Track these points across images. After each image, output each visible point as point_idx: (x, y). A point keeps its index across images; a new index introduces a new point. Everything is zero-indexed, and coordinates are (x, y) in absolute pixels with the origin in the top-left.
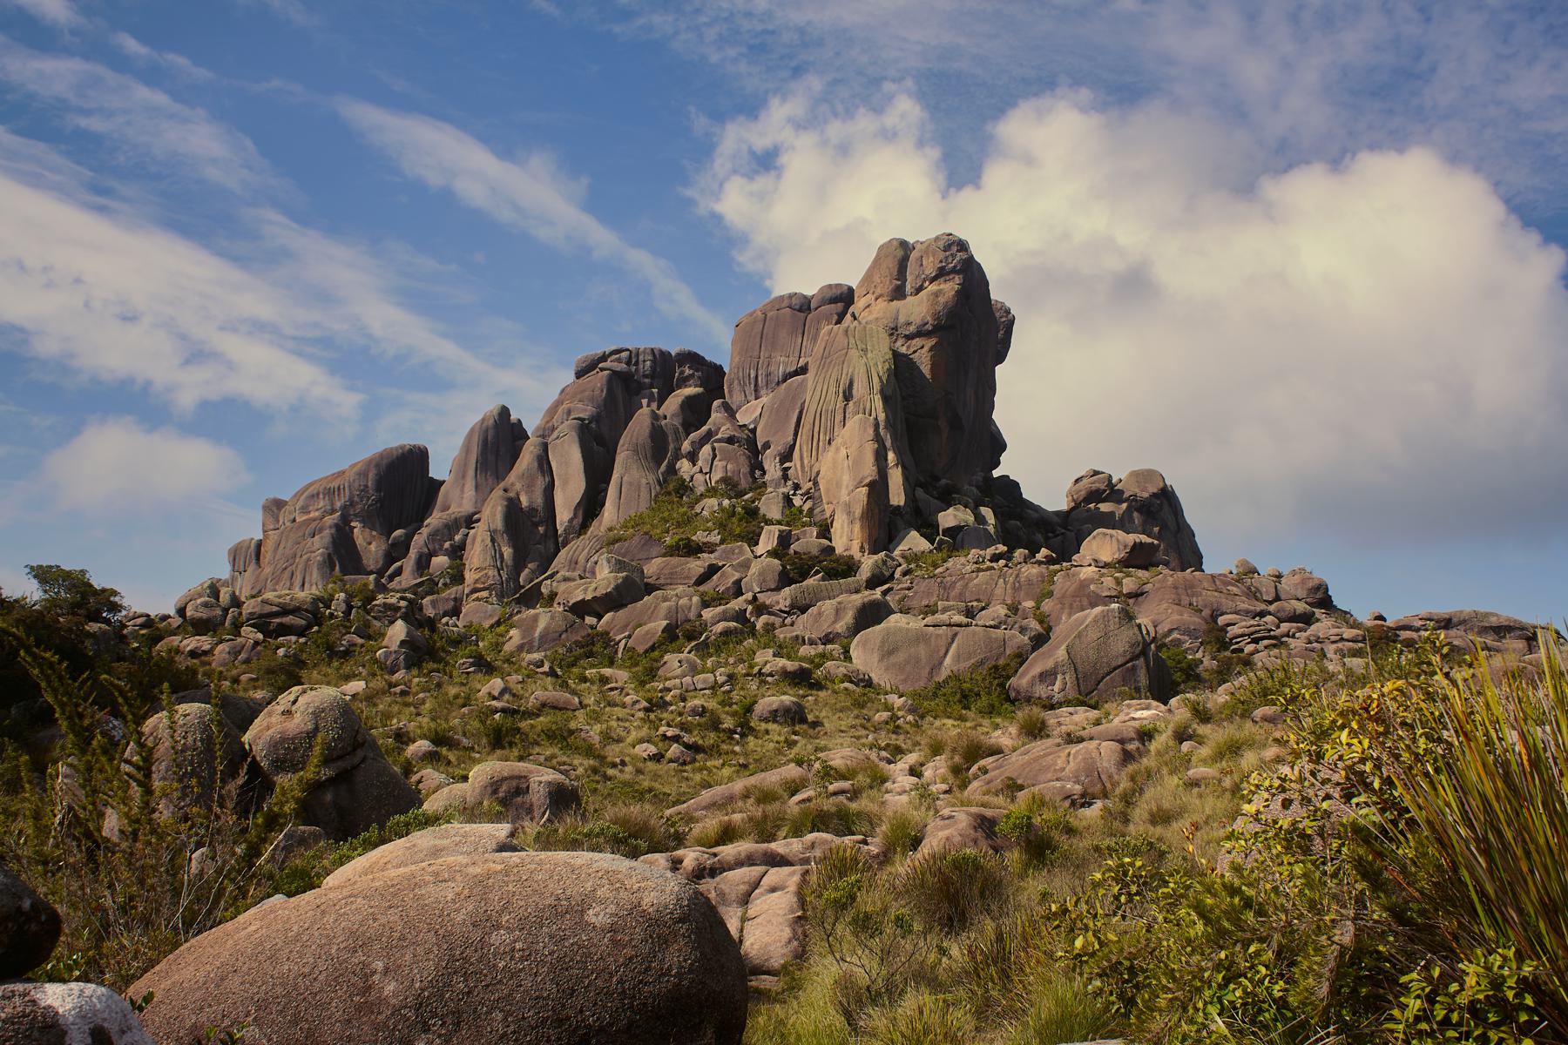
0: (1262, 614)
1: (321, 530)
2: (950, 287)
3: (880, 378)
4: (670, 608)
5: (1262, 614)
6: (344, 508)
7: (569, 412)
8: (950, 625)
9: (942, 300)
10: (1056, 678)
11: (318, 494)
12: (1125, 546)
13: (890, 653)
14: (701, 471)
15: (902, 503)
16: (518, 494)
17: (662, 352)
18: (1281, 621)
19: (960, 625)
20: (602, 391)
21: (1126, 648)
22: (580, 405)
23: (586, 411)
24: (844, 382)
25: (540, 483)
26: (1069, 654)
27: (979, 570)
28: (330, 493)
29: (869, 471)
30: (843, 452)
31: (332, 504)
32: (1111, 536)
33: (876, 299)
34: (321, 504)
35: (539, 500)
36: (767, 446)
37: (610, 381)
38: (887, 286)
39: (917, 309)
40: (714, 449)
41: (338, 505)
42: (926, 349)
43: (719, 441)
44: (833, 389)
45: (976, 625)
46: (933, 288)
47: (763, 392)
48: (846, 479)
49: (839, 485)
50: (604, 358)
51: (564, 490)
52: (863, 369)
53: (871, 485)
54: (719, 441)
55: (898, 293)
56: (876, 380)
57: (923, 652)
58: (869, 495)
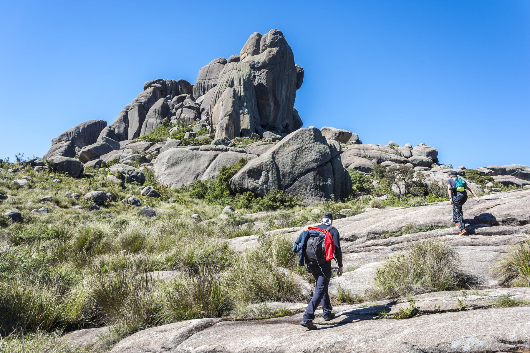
0: (405, 162)
1: (62, 147)
2: (275, 50)
3: (244, 80)
4: (116, 157)
5: (405, 162)
6: (72, 140)
7: (137, 100)
8: (216, 150)
9: (272, 54)
10: (261, 174)
11: (64, 135)
12: (335, 135)
13: (174, 164)
14: (176, 118)
15: (249, 128)
16: (114, 129)
17: (175, 81)
18: (415, 165)
19: (221, 150)
20: (151, 93)
21: (318, 157)
22: (142, 98)
23: (143, 100)
24: (230, 81)
25: (123, 126)
26: (274, 158)
27: (265, 144)
28: (68, 134)
29: (230, 108)
30: (221, 103)
31: (68, 138)
32: (329, 130)
33: (248, 55)
34: (65, 138)
35: (122, 130)
36: (203, 109)
37: (154, 91)
38: (251, 50)
39: (262, 57)
40: (182, 110)
41: (70, 138)
42: (265, 72)
43: (186, 107)
44: (225, 84)
45: (232, 150)
46: (269, 49)
47: (205, 92)
48: (222, 114)
49: (218, 117)
50: (154, 82)
51: (131, 127)
52: (237, 76)
53: (230, 115)
54: (186, 107)
55: (256, 52)
56: (242, 81)
57: (193, 165)
58: (229, 120)
